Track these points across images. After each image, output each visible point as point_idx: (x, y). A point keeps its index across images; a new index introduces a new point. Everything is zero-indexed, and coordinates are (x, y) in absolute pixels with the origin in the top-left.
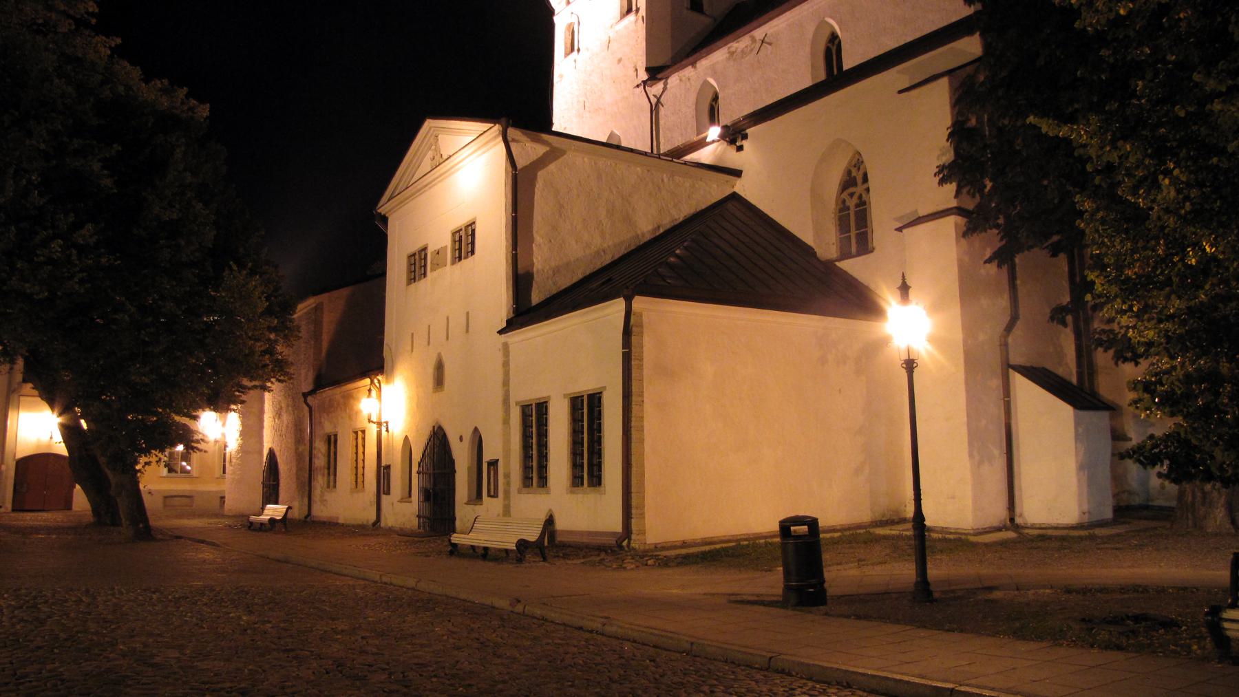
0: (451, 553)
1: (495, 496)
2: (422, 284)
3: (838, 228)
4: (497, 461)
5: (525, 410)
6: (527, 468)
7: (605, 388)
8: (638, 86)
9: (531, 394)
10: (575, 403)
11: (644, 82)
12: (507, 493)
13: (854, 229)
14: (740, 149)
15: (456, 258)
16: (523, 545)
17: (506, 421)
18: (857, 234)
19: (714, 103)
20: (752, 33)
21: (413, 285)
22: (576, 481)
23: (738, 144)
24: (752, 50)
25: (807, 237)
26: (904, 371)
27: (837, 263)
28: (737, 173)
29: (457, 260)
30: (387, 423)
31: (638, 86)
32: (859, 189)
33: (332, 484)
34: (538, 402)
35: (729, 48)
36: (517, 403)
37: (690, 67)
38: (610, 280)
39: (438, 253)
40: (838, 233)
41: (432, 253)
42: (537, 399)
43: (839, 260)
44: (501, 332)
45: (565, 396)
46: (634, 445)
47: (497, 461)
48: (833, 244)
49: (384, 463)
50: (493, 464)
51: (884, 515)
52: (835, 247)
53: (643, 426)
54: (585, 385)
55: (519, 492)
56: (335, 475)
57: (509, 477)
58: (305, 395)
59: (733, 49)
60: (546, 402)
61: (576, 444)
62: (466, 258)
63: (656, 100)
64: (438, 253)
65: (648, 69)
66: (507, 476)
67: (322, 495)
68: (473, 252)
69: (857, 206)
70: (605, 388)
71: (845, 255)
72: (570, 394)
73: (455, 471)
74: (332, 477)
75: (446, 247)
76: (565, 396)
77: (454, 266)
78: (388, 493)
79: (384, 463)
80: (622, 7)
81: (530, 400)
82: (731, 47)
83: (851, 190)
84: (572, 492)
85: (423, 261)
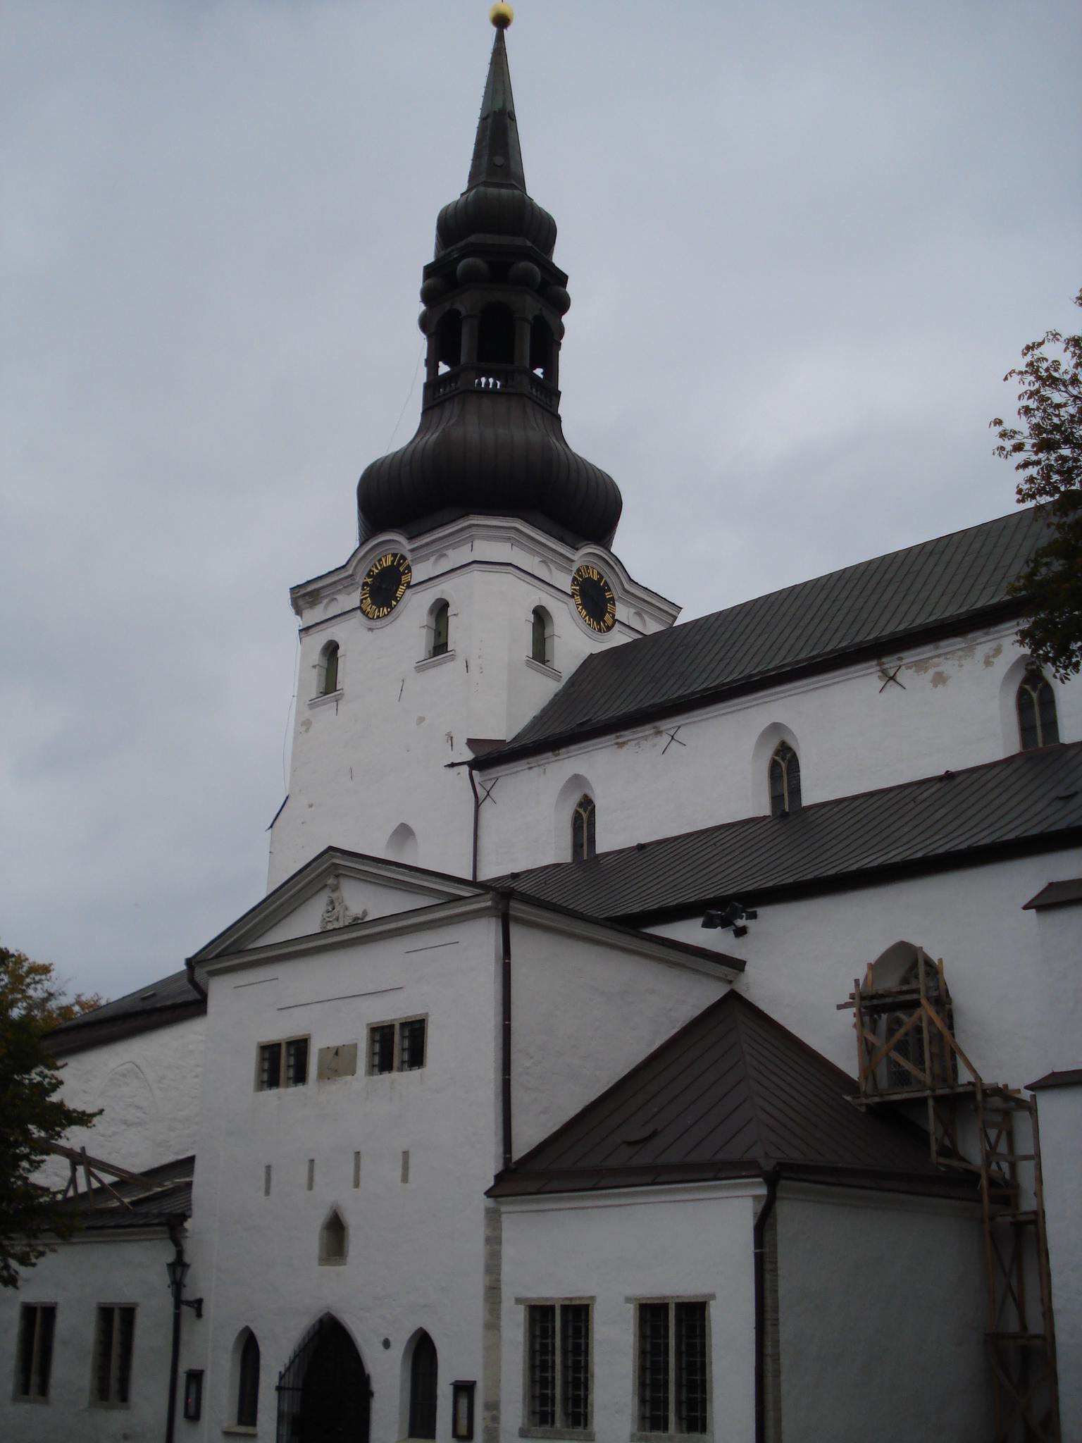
2: (288, 1094)
5: (540, 1314)
7: (713, 1297)
8: (452, 765)
11: (469, 764)
15: (373, 1066)
17: (493, 1324)
19: (581, 811)
20: (657, 724)
21: (271, 1094)
23: (740, 923)
24: (655, 745)
28: (739, 965)
29: (376, 1069)
31: (452, 765)
33: (34, 1388)
34: (567, 1303)
35: (618, 737)
37: (550, 754)
41: (321, 1051)
42: (566, 1299)
44: (488, 1194)
49: (183, 1369)
50: (464, 1389)
55: (523, 1434)
59: (620, 740)
62: (401, 1069)
63: (486, 794)
64: (337, 1053)
65: (472, 743)
66: (493, 1407)
70: (713, 1297)
72: (636, 1299)
73: (371, 1394)
74: (35, 1379)
75: (356, 1045)
76: (628, 1300)
78: (194, 1416)
82: (621, 736)
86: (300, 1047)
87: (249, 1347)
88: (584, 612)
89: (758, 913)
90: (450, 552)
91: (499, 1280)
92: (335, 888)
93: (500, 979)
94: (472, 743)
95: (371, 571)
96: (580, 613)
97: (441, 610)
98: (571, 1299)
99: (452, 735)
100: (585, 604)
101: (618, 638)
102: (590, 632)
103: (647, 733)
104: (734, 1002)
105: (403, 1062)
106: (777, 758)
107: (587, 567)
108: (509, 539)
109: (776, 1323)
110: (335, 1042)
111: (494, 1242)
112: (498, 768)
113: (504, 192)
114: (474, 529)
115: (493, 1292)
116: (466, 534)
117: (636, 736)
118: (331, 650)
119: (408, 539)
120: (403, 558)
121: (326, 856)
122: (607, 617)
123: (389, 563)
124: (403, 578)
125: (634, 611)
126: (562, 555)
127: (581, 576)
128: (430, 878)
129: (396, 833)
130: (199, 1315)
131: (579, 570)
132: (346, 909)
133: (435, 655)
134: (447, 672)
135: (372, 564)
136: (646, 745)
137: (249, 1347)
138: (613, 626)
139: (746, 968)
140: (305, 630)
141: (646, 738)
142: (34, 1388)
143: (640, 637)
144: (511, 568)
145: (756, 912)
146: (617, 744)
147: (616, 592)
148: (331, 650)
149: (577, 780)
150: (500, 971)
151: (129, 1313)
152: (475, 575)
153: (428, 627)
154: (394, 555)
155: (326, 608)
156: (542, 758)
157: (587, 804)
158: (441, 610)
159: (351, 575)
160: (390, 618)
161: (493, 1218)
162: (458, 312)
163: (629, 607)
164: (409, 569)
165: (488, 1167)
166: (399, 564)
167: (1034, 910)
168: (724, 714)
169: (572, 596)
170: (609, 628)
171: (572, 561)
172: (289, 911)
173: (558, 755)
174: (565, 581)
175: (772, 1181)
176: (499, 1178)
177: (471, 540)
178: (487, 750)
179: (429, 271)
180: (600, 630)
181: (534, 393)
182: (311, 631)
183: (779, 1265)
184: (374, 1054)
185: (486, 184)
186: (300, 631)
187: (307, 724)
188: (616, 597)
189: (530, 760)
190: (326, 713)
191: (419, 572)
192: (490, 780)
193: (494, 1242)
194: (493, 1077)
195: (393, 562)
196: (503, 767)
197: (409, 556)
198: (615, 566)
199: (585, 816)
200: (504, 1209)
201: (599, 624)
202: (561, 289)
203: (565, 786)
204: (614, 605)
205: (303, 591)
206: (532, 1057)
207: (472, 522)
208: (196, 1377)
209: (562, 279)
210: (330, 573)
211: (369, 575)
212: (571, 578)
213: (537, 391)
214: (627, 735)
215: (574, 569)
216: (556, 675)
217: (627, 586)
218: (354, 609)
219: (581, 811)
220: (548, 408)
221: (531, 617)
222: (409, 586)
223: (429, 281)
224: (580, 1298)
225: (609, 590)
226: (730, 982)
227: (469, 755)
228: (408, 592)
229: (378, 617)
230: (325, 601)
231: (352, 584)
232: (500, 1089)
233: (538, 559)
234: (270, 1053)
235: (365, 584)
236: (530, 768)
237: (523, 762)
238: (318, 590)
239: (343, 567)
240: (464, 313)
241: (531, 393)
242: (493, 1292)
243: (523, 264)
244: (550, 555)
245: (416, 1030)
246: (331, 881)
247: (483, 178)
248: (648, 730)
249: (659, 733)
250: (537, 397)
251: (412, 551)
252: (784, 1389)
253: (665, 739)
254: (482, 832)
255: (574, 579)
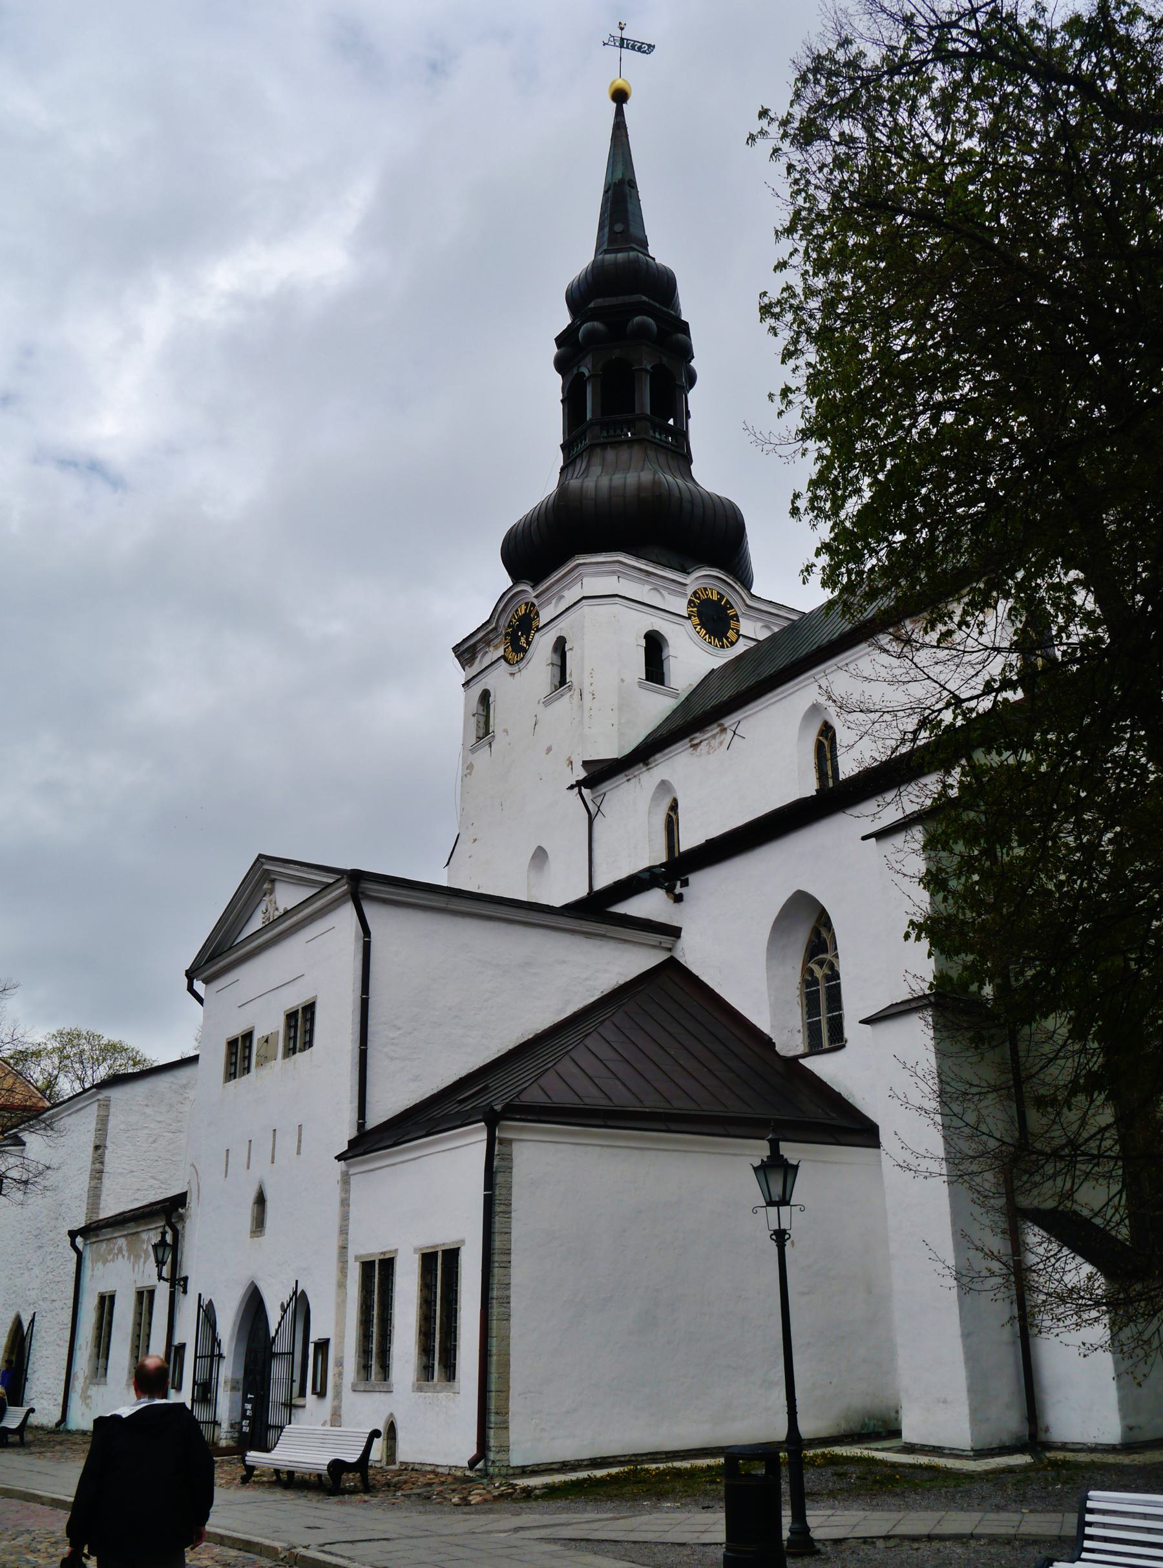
0: (245, 1480)
1: (321, 1394)
3: (805, 1009)
4: (328, 1340)
5: (367, 1267)
6: (365, 1352)
7: (463, 1242)
8: (571, 787)
9: (373, 1249)
10: (428, 1259)
11: (579, 784)
12: (338, 1395)
13: (825, 1011)
14: (678, 899)
16: (337, 1466)
17: (342, 1285)
18: (829, 1018)
19: (672, 814)
21: (233, 1082)
22: (426, 1372)
23: (678, 890)
24: (721, 743)
25: (762, 1021)
26: (774, 1244)
27: (801, 1061)
28: (674, 932)
29: (291, 1052)
30: (186, 1279)
32: (828, 956)
34: (382, 1257)
36: (357, 1258)
37: (641, 765)
38: (486, 1088)
39: (267, 1041)
40: (805, 1017)
43: (804, 1056)
44: (339, 1158)
45: (415, 1251)
46: (494, 1324)
47: (328, 1340)
48: (799, 1031)
49: (176, 1342)
51: (864, 1425)
52: (801, 1035)
53: (508, 1297)
54: (440, 1238)
56: (107, 1358)
57: (341, 1365)
58: (73, 1234)
60: (393, 1258)
61: (426, 1319)
62: (301, 1050)
64: (267, 1041)
65: (586, 764)
66: (340, 1364)
67: (85, 1389)
68: (309, 1044)
69: (828, 978)
70: (463, 1242)
71: (815, 1049)
77: (287, 1060)
79: (176, 1342)
80: (553, 676)
81: (371, 1255)
83: (821, 956)
84: (420, 1389)
85: (247, 1051)
86: (248, 1036)
87: (207, 1315)
88: (703, 632)
89: (690, 881)
90: (566, 593)
91: (347, 1239)
92: (271, 891)
93: (360, 956)
94: (586, 764)
95: (511, 621)
96: (698, 632)
97: (560, 646)
98: (383, 1253)
99: (573, 759)
100: (703, 624)
101: (741, 647)
102: (710, 648)
103: (714, 732)
104: (673, 969)
105: (305, 1043)
106: (821, 738)
107: (705, 589)
108: (614, 572)
109: (507, 1265)
110: (266, 1033)
111: (345, 1203)
112: (604, 784)
113: (620, 256)
114: (580, 568)
115: (344, 1248)
116: (575, 574)
117: (706, 736)
118: (485, 697)
119: (532, 587)
120: (533, 605)
121: (258, 865)
122: (731, 634)
123: (523, 612)
124: (534, 624)
125: (762, 624)
126: (673, 581)
127: (699, 598)
128: (313, 871)
129: (534, 856)
130: (185, 1292)
131: (695, 593)
132: (277, 909)
133: (561, 687)
134: (565, 703)
135: (511, 615)
136: (715, 743)
137: (207, 1315)
138: (737, 641)
139: (683, 934)
140: (466, 684)
141: (714, 736)
142: (101, 1371)
143: (755, 643)
144: (617, 599)
145: (687, 879)
146: (691, 746)
147: (739, 608)
148: (485, 697)
149: (664, 786)
150: (361, 950)
151: (151, 1293)
152: (586, 608)
153: (552, 664)
154: (527, 604)
155: (481, 661)
156: (634, 771)
157: (674, 807)
158: (560, 646)
159: (495, 629)
160: (525, 661)
161: (346, 1180)
162: (583, 374)
163: (755, 621)
164: (537, 614)
165: (346, 1132)
166: (531, 611)
167: (874, 839)
168: (773, 704)
169: (689, 618)
170: (732, 644)
171: (685, 585)
172: (248, 915)
173: (647, 765)
174: (680, 605)
175: (492, 1121)
176: (352, 1143)
177: (580, 578)
178: (599, 767)
179: (561, 341)
180: (722, 647)
181: (657, 436)
182: (471, 684)
183: (514, 1207)
184: (290, 1038)
185: (606, 252)
186: (463, 685)
187: (470, 767)
188: (739, 614)
189: (627, 773)
190: (483, 753)
191: (545, 616)
192: (600, 796)
193: (345, 1203)
194: (350, 1048)
195: (526, 610)
196: (608, 783)
197: (535, 601)
198: (734, 585)
199: (674, 817)
200: (352, 1171)
201: (720, 640)
202: (681, 336)
203: (655, 793)
204: (738, 621)
205: (462, 649)
206: (399, 1029)
207: (578, 562)
208: (182, 1346)
209: (684, 328)
210: (478, 629)
211: (509, 626)
212: (686, 602)
213: (660, 435)
214: (699, 737)
215: (690, 591)
216: (676, 696)
217: (749, 602)
218: (499, 659)
219: (672, 814)
220: (677, 450)
221: (643, 642)
222: (538, 629)
223: (562, 349)
224: (390, 1252)
225: (732, 607)
226: (670, 950)
227: (582, 774)
228: (537, 634)
229: (517, 662)
230: (479, 656)
231: (497, 637)
232: (357, 1059)
233: (647, 587)
234: (232, 1044)
235: (507, 634)
236: (628, 780)
237: (623, 774)
238: (474, 646)
239: (488, 622)
240: (587, 374)
241: (655, 438)
242: (344, 1248)
243: (638, 319)
244: (660, 582)
245: (309, 1009)
246: (266, 886)
247: (605, 247)
248: (714, 729)
249: (724, 730)
250: (661, 440)
251: (536, 597)
252: (514, 1333)
253: (730, 734)
254: (595, 846)
255: (690, 602)
